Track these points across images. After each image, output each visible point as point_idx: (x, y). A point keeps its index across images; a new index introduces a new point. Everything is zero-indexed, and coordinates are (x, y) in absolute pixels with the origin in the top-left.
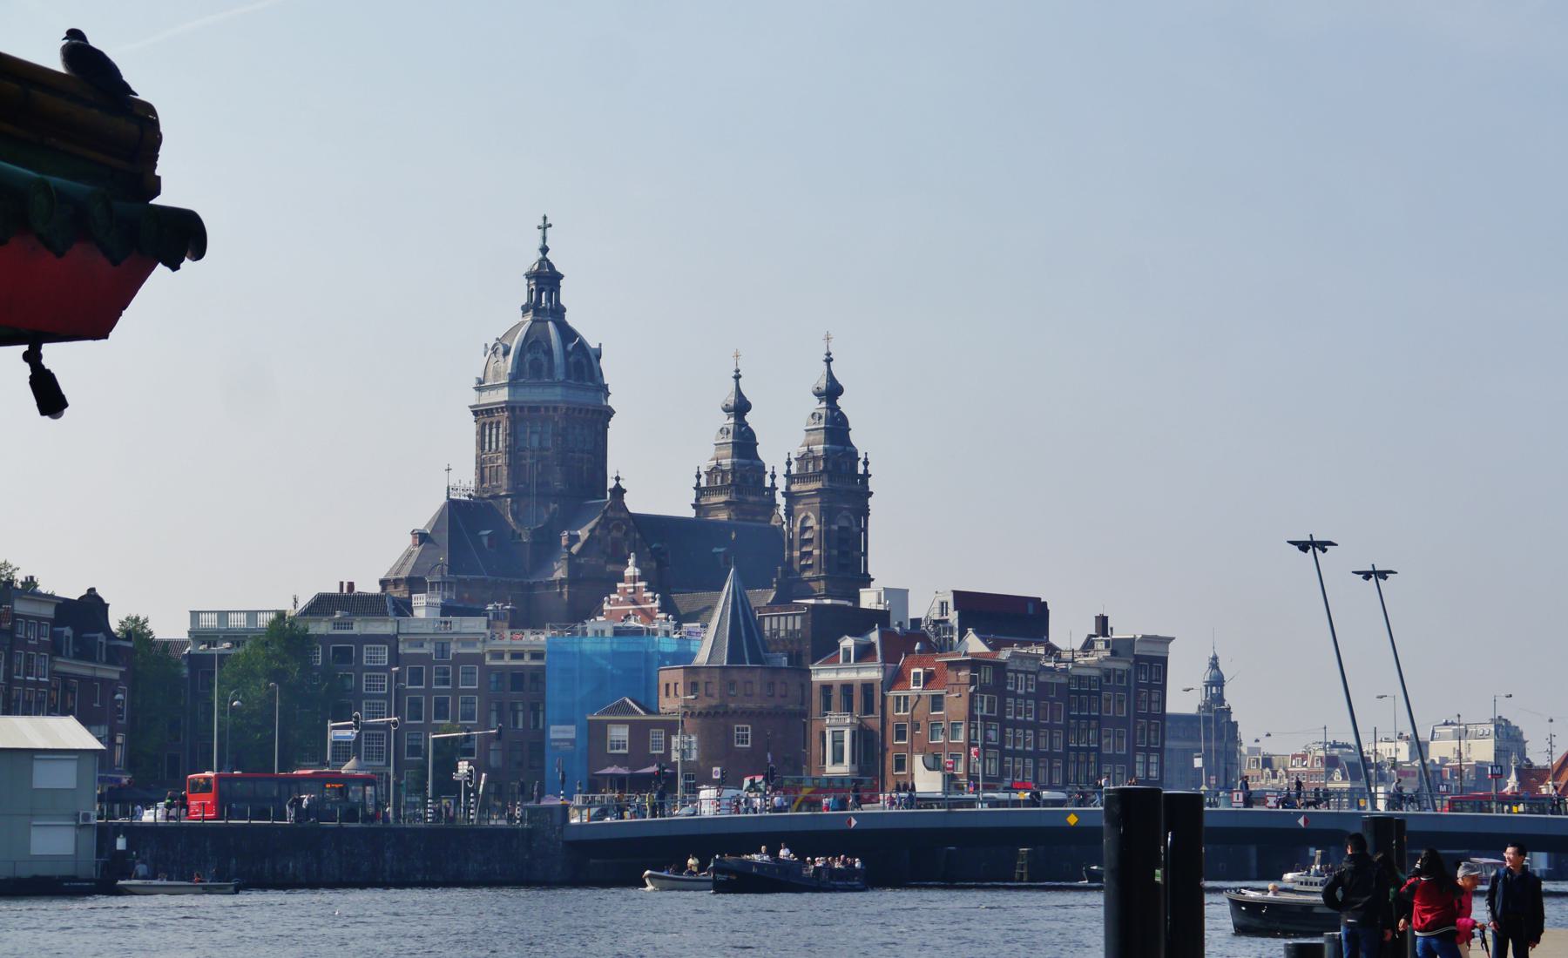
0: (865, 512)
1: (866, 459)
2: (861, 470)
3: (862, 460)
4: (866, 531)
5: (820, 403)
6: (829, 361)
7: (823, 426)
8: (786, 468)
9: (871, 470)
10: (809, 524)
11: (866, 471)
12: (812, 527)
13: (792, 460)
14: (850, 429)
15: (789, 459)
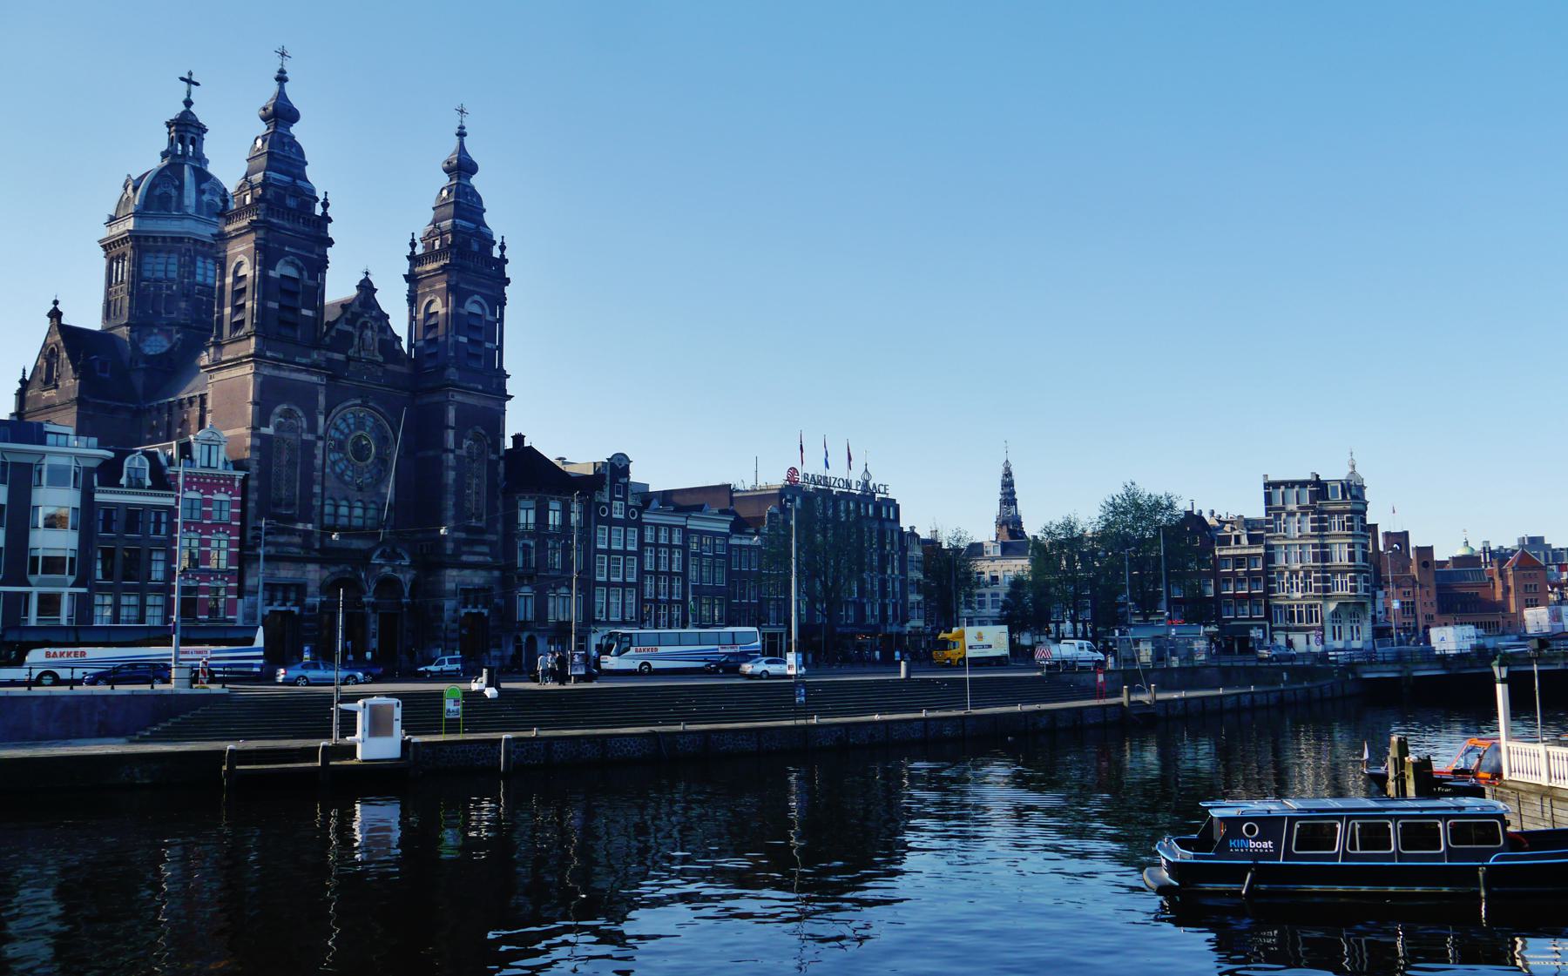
0: (502, 302)
1: (503, 243)
2: (496, 253)
3: (498, 244)
4: (501, 320)
5: (451, 180)
6: (461, 134)
7: (452, 200)
8: (410, 250)
9: (507, 254)
10: (432, 310)
11: (502, 256)
12: (437, 312)
13: (417, 241)
14: (485, 211)
15: (413, 240)
